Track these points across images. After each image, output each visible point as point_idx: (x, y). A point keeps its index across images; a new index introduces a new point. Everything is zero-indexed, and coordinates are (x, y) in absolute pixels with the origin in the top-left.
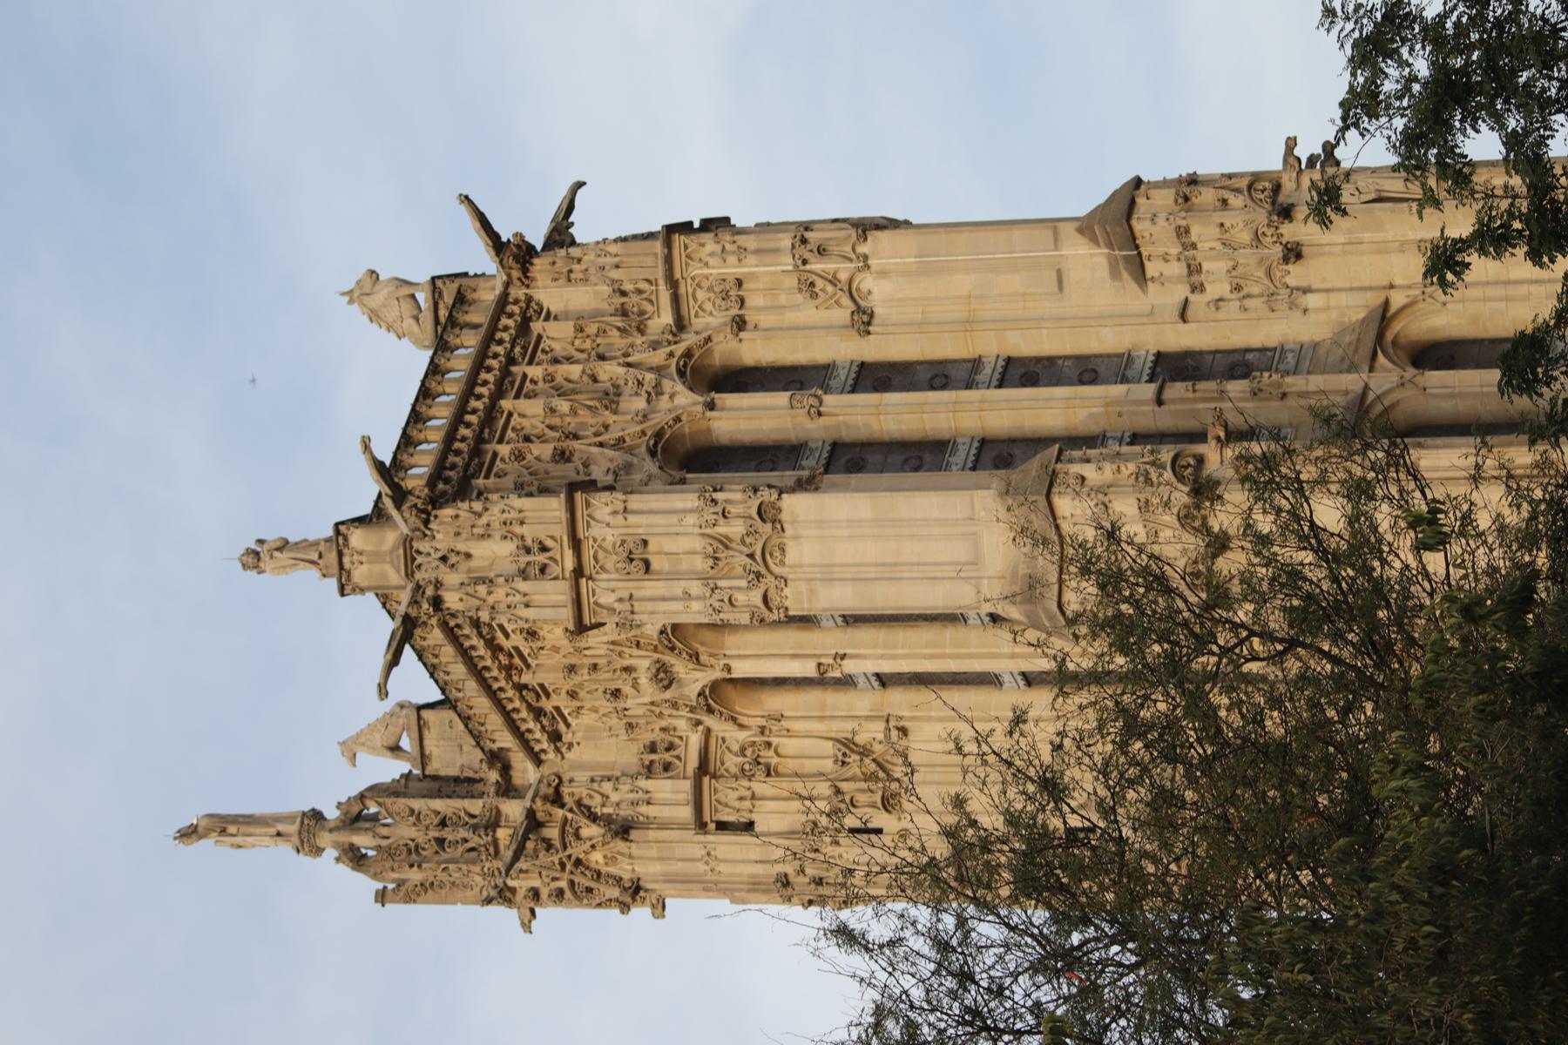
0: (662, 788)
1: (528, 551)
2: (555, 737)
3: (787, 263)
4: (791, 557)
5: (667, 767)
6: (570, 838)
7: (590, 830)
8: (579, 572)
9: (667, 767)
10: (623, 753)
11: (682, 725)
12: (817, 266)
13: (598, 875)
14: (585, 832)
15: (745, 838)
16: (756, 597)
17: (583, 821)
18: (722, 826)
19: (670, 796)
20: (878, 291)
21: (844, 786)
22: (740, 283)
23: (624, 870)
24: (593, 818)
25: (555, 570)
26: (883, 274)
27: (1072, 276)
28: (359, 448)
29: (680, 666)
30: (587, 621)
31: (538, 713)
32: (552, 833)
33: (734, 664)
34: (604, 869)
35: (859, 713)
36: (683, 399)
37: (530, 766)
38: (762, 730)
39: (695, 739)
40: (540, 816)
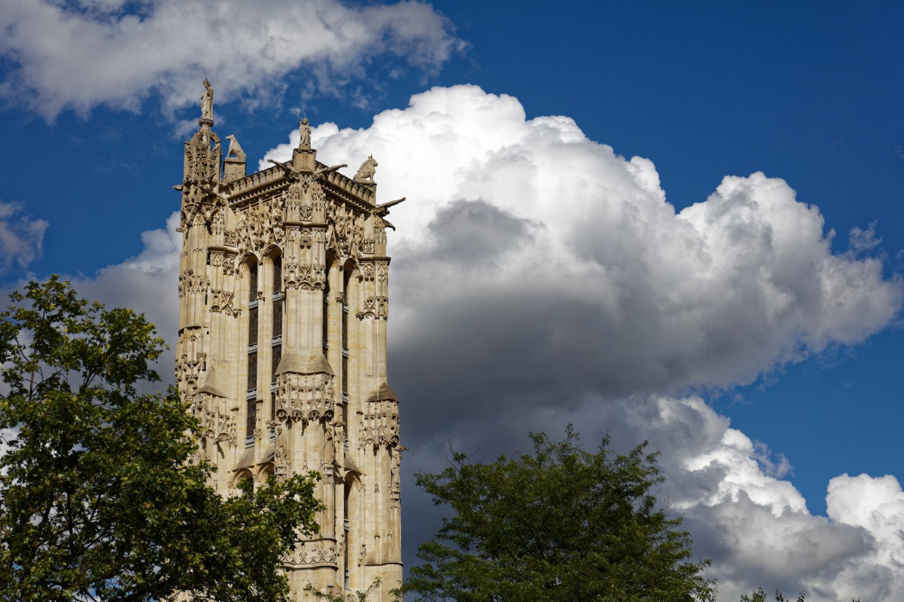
2: (237, 206)
3: (378, 294)
7: (208, 214)
8: (301, 227)
10: (231, 227)
12: (377, 303)
13: (194, 214)
15: (205, 261)
16: (292, 279)
18: (209, 255)
19: (218, 240)
20: (369, 320)
22: (372, 280)
23: (195, 222)
24: (212, 215)
26: (373, 323)
27: (371, 380)
28: (344, 163)
31: (246, 203)
35: (243, 301)
36: (343, 260)
38: (238, 271)
39: (236, 249)
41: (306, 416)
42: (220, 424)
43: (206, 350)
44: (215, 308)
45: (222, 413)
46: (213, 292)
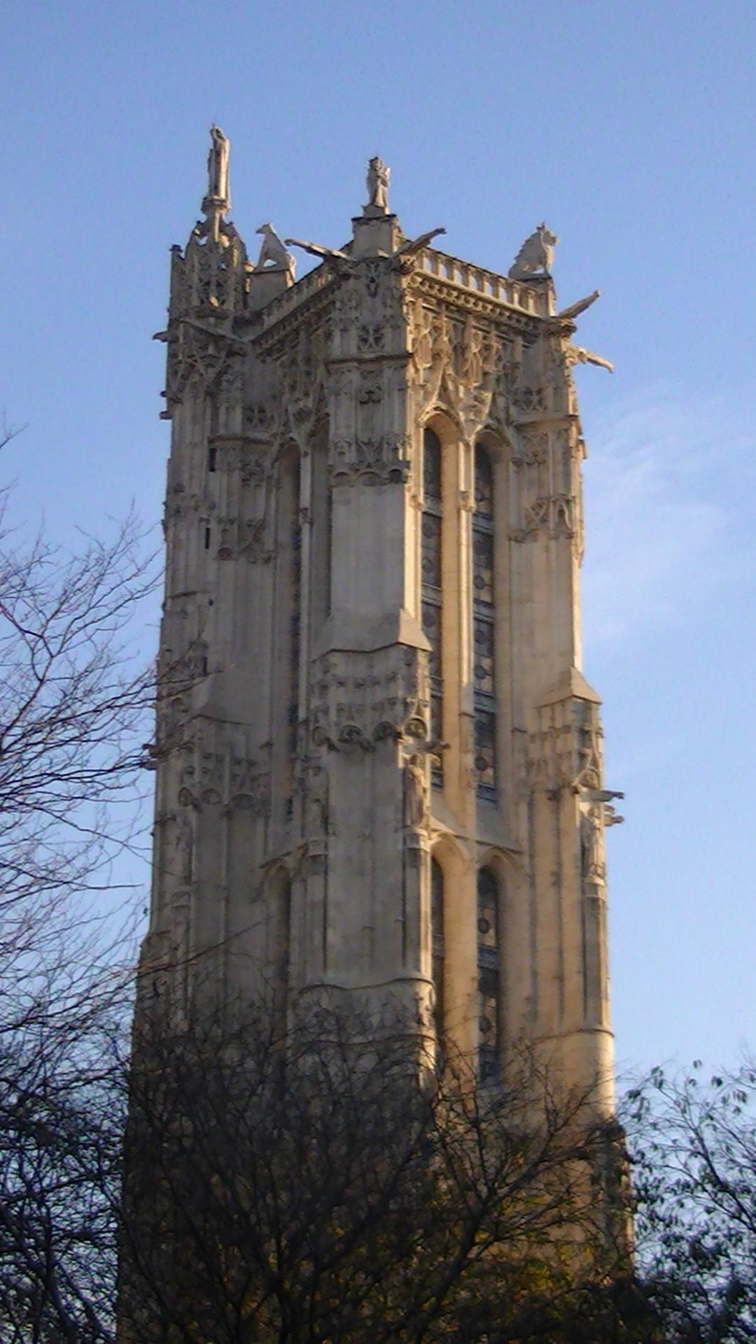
0: (238, 415)
1: (376, 331)
2: (269, 352)
4: (369, 491)
5: (250, 420)
6: (208, 361)
7: (211, 374)
8: (361, 361)
9: (250, 420)
11: (276, 428)
14: (210, 370)
17: (217, 369)
18: (212, 452)
21: (235, 526)
24: (220, 375)
25: (365, 349)
26: (547, 550)
29: (308, 426)
30: (331, 367)
31: (281, 342)
32: (211, 350)
33: (309, 459)
34: (189, 383)
37: (251, 338)
40: (221, 344)
41: (368, 735)
42: (234, 777)
43: (207, 636)
44: (224, 554)
45: (241, 754)
46: (220, 522)
